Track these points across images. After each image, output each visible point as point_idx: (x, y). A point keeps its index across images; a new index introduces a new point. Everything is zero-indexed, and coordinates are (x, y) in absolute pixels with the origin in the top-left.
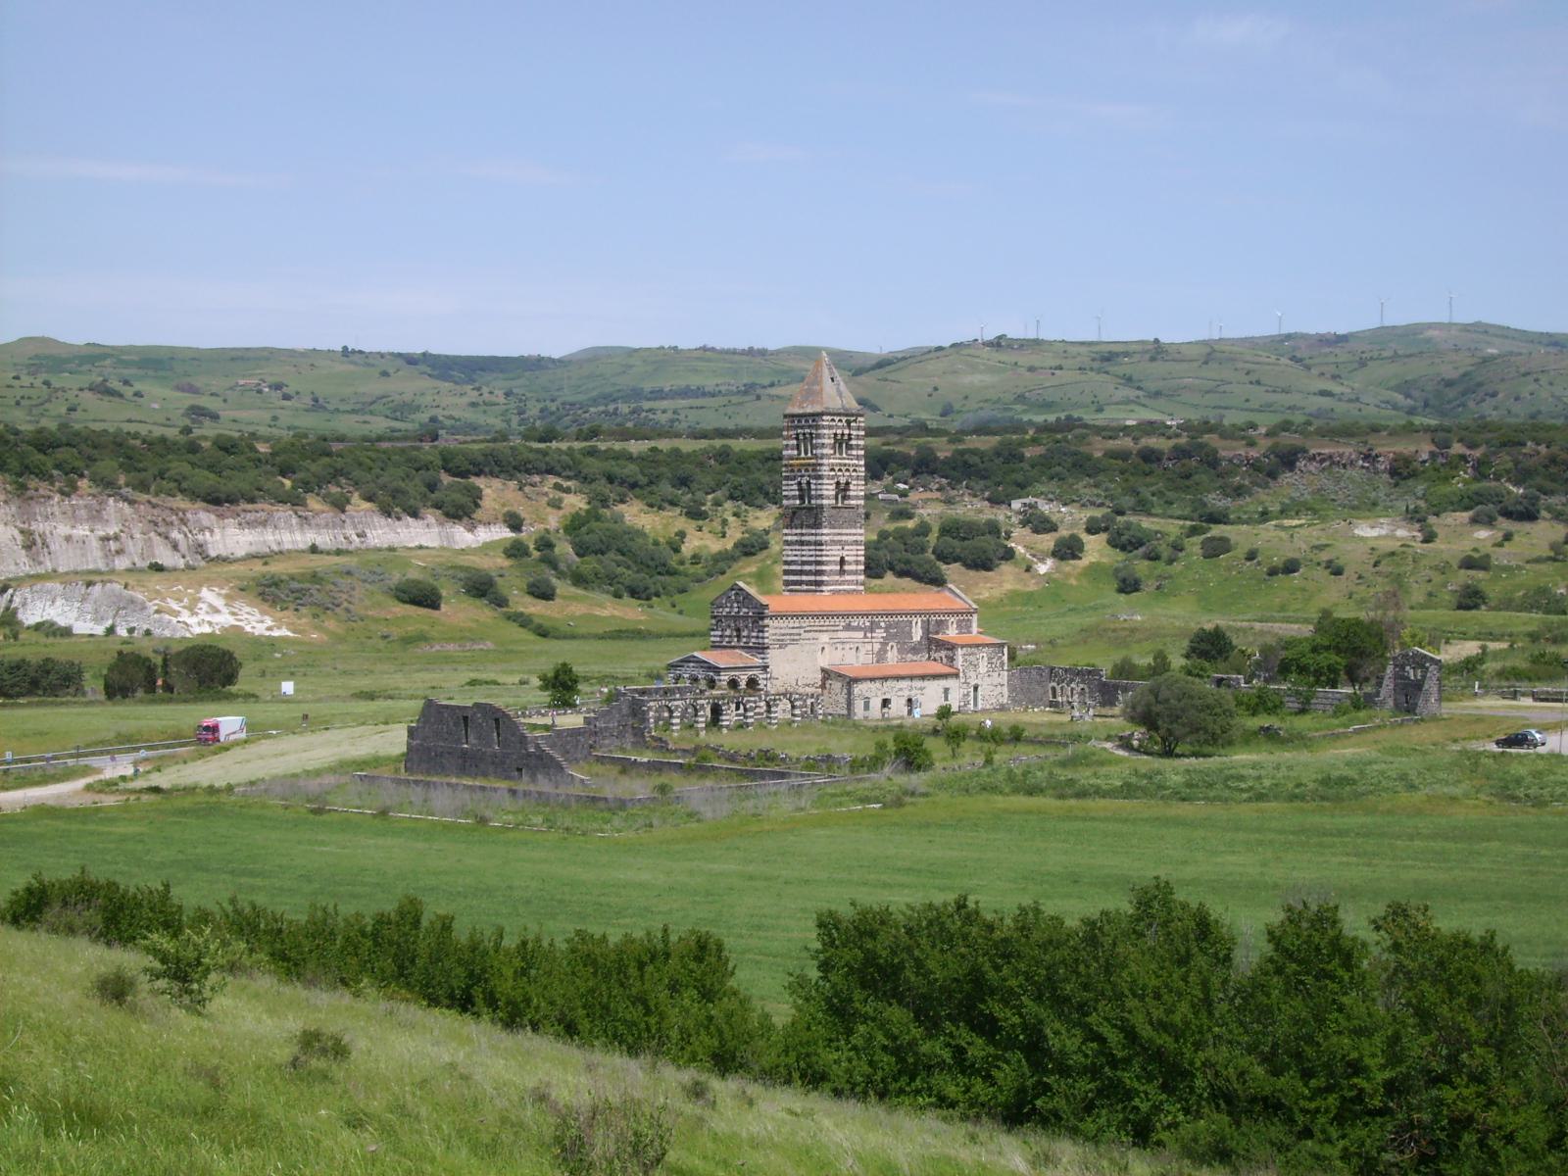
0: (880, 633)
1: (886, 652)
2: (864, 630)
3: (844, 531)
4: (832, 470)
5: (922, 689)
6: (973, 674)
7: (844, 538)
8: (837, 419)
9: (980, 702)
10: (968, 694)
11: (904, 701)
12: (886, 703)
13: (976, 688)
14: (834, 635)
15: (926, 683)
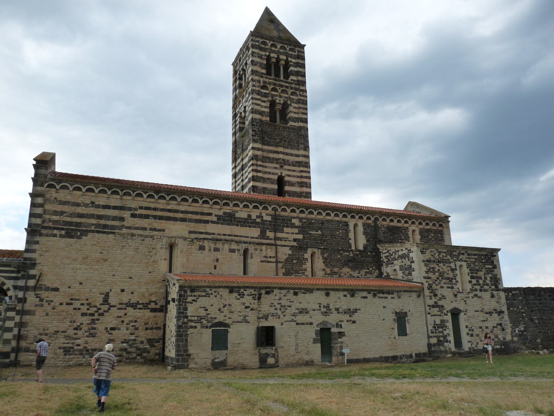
0: (290, 235)
1: (302, 261)
2: (262, 225)
3: (281, 149)
4: (264, 87)
5: (351, 312)
6: (447, 292)
7: (281, 156)
8: (270, 43)
9: (465, 339)
10: (442, 325)
11: (311, 333)
12: (266, 337)
13: (455, 314)
14: (201, 228)
15: (356, 302)
